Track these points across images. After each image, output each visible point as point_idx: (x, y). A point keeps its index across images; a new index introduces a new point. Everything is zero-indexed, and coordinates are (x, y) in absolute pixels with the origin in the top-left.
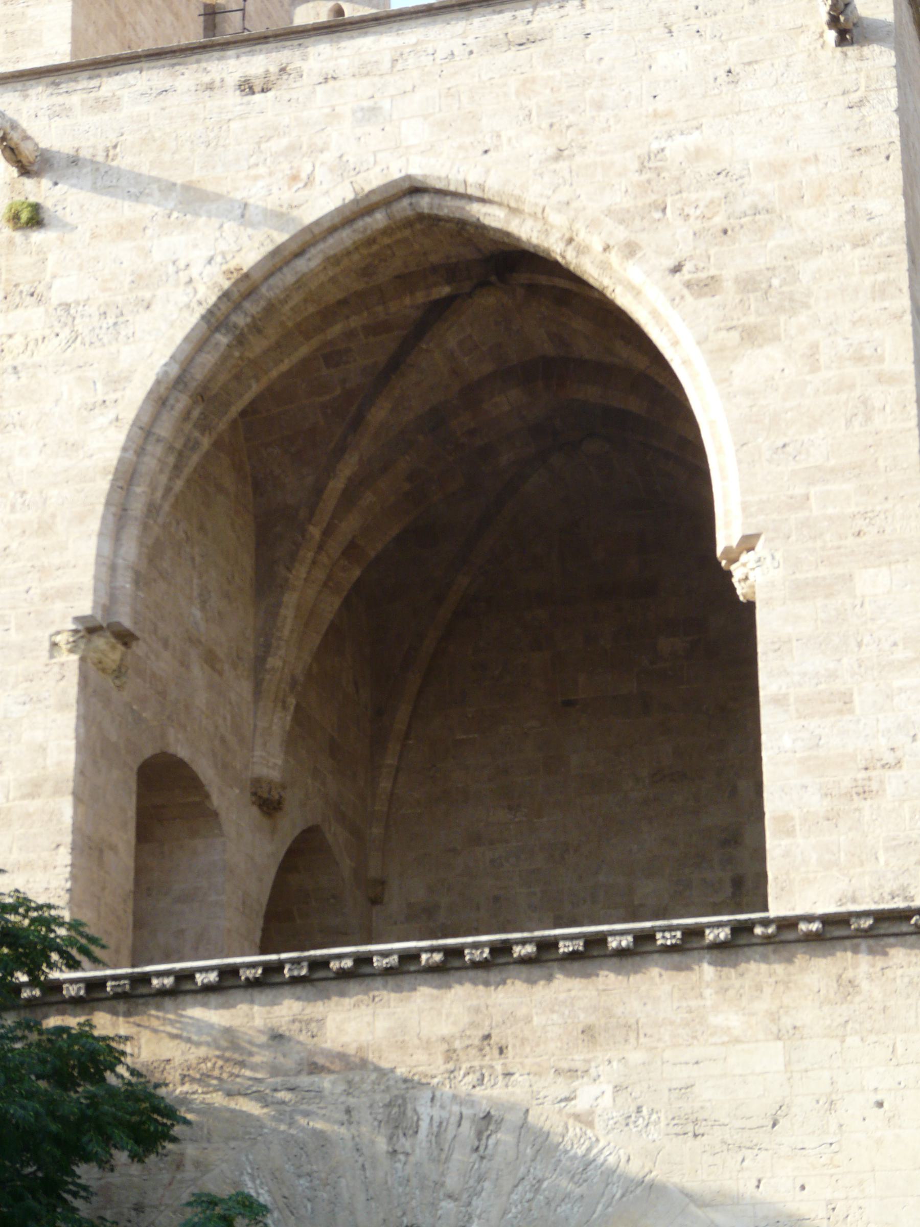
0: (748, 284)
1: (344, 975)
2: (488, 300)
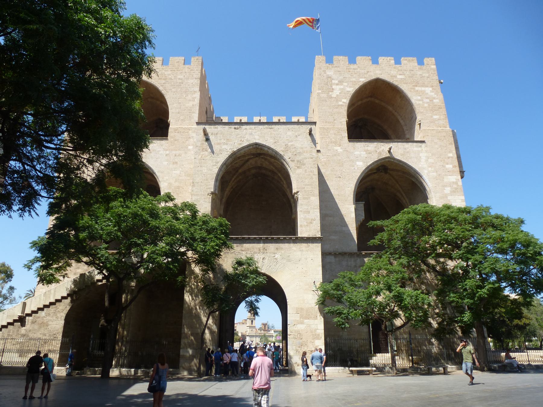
0: (298, 161)
1: (246, 239)
2: (257, 158)
